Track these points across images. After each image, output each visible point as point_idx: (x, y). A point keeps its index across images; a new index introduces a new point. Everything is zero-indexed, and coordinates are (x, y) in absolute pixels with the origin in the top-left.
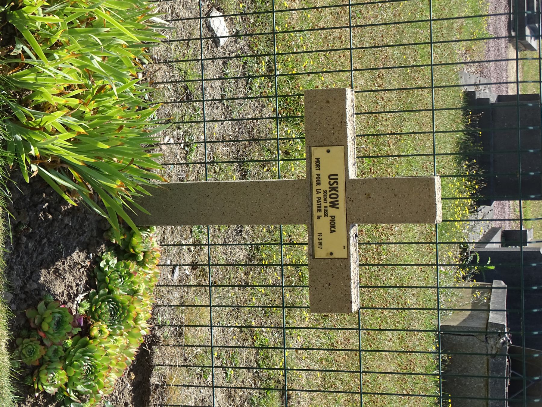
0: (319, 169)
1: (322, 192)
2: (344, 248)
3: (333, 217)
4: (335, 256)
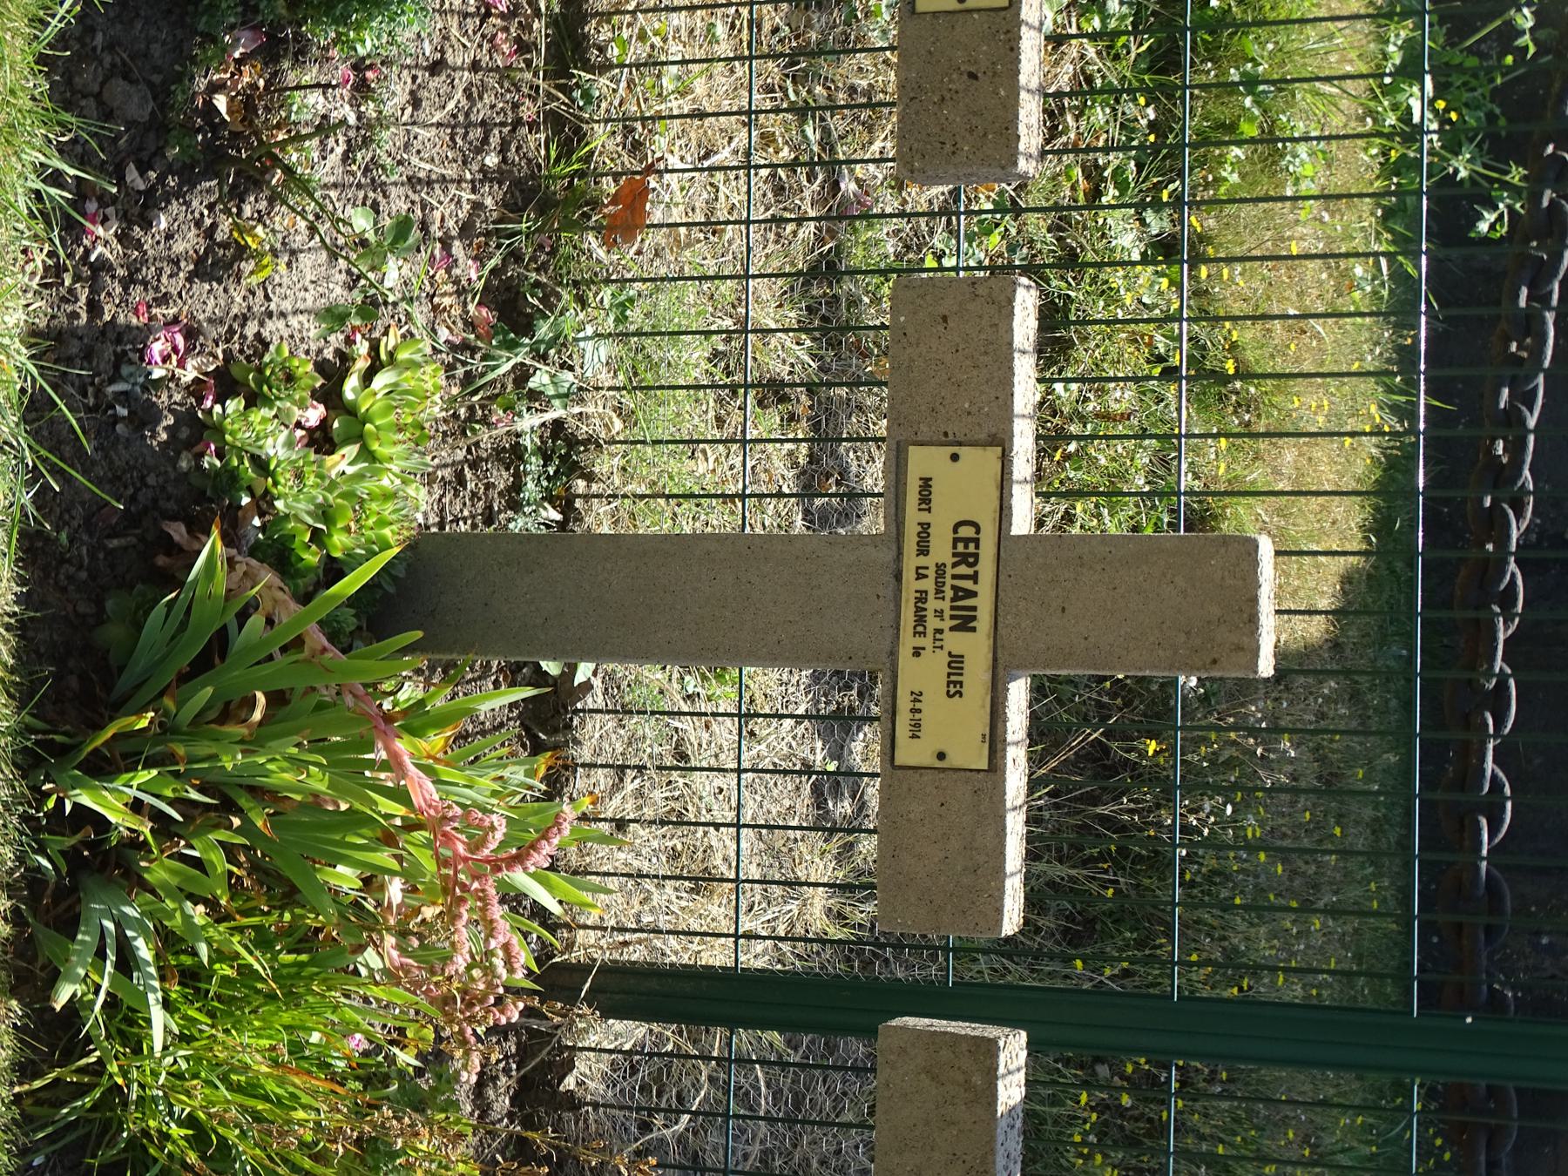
0: (929, 510)
1: (931, 573)
3: (956, 663)
4: (955, 760)
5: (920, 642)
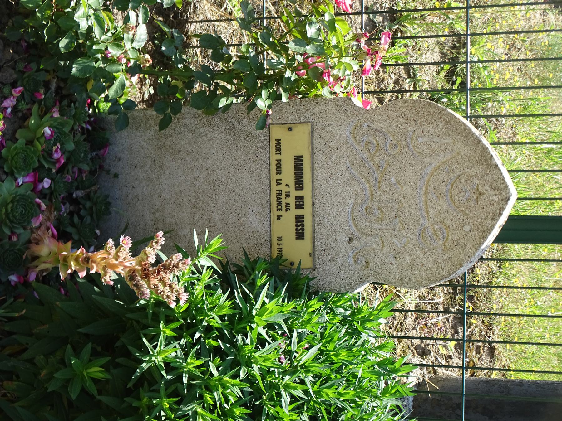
0: (280, 154)
2: (310, 255)
5: (280, 213)
